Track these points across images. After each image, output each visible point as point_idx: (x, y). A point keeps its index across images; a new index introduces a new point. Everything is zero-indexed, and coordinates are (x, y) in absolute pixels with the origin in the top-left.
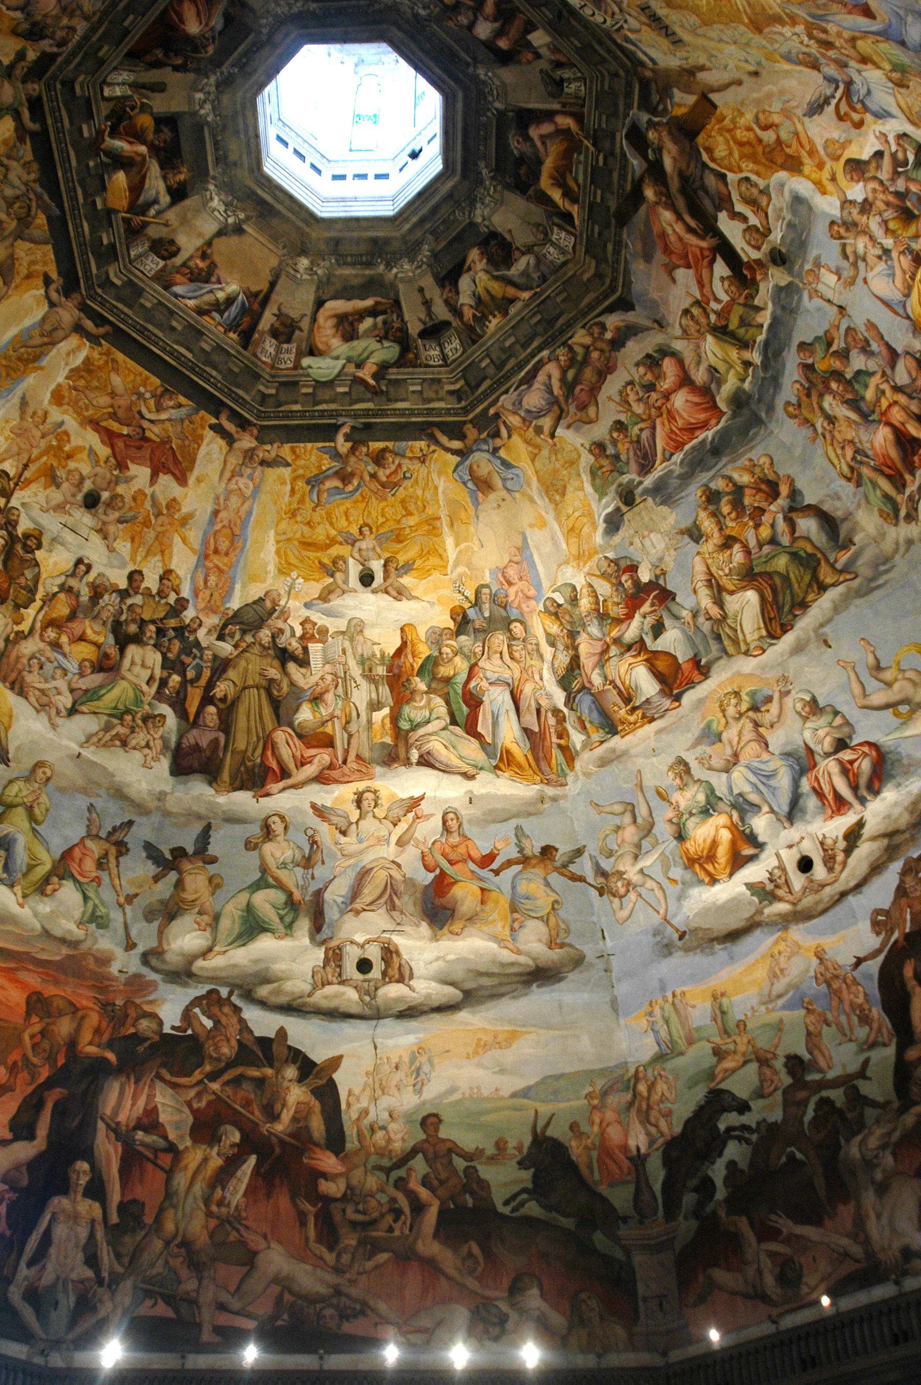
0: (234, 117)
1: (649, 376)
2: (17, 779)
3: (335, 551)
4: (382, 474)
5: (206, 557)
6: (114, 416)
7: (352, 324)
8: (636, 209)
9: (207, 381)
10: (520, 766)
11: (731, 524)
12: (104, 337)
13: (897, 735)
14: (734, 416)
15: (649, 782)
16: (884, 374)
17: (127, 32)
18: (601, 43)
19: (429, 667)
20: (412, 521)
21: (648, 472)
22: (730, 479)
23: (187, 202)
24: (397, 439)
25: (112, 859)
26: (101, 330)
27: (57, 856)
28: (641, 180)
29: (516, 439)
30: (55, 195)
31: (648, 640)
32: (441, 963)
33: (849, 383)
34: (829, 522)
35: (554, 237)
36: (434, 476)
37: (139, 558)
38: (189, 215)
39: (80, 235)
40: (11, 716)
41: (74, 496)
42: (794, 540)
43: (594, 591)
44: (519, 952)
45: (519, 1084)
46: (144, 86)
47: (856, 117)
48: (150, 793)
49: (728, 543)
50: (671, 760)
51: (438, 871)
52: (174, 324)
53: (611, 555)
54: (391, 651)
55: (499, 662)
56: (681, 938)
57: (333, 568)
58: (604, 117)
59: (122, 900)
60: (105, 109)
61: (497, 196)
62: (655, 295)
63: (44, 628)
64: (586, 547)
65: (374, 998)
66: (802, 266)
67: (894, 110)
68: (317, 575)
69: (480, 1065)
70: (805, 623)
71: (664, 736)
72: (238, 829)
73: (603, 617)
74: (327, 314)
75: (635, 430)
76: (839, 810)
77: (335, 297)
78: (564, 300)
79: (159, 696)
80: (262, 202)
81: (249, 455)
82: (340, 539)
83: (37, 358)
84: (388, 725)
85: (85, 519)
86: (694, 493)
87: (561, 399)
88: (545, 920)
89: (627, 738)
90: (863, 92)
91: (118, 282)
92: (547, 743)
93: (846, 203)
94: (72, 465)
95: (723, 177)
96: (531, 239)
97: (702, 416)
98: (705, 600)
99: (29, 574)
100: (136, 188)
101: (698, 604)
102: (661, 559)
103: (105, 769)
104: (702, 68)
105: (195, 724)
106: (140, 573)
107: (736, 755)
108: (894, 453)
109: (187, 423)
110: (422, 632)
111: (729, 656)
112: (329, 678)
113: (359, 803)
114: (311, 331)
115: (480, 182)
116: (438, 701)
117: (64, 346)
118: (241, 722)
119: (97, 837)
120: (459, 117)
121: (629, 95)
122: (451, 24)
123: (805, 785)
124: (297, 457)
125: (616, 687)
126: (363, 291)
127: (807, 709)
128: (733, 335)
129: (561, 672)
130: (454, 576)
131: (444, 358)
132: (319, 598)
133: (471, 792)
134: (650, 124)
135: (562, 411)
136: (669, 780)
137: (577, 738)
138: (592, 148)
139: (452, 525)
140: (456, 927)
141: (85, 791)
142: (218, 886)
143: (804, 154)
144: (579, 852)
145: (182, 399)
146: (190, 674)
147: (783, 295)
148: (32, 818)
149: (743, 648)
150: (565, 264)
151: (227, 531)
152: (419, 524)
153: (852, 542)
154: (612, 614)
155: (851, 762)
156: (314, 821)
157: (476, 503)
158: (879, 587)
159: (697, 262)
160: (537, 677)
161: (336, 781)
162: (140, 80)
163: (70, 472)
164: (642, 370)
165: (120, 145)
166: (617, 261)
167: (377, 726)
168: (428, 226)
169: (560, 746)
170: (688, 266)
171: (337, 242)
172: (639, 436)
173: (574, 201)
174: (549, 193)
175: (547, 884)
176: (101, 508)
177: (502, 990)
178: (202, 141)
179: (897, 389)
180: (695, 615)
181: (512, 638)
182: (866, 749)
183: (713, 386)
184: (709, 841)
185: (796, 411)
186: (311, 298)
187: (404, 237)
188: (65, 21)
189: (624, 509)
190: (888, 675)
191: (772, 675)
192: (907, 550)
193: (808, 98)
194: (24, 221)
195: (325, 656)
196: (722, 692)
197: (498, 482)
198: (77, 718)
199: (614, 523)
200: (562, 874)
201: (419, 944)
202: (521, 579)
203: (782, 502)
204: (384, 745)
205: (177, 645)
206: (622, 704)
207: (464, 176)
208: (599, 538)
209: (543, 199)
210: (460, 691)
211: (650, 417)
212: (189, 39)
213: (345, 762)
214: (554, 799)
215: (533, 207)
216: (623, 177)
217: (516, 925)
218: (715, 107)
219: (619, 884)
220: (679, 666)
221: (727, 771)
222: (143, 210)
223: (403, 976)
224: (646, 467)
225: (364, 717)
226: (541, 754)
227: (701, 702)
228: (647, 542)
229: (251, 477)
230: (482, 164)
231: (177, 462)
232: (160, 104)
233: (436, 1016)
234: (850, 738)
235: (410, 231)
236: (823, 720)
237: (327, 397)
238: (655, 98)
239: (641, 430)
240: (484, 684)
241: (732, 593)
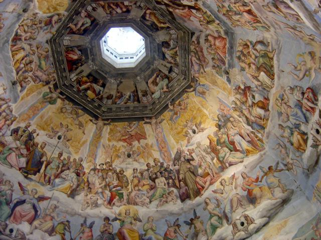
0: (101, 64)
2: (145, 224)
3: (184, 130)
4: (182, 107)
5: (161, 150)
6: (123, 136)
9: (137, 115)
10: (252, 151)
11: (246, 61)
12: (111, 122)
14: (228, 37)
15: (278, 135)
17: (64, 69)
19: (218, 142)
20: (195, 112)
22: (239, 51)
23: (107, 86)
25: (178, 230)
26: (109, 121)
27: (163, 236)
29: (200, 78)
30: (79, 105)
31: (254, 101)
32: (259, 213)
34: (261, 42)
35: (171, 33)
37: (146, 160)
38: (110, 87)
39: (90, 108)
40: (137, 211)
42: (259, 53)
44: (276, 199)
45: (293, 235)
46: (79, 74)
48: (179, 209)
49: (249, 65)
50: (277, 126)
52: (122, 109)
53: (234, 88)
54: (209, 144)
56: (308, 171)
57: (186, 135)
59: (185, 238)
60: (75, 83)
63: (134, 188)
65: (248, 231)
69: (281, 235)
70: (276, 70)
71: (273, 121)
72: (200, 207)
73: (243, 103)
75: (216, 57)
76: (314, 111)
77: (149, 79)
79: (169, 186)
80: (121, 74)
81: (156, 123)
83: (100, 136)
85: (130, 160)
86: (236, 60)
88: (279, 186)
91: (106, 110)
94: (120, 151)
97: (223, 42)
98: (256, 83)
99: (125, 179)
100: (94, 91)
102: (242, 81)
103: (165, 210)
105: (180, 188)
106: (149, 163)
107: (287, 115)
113: (222, 184)
114: (150, 90)
115: (152, 35)
116: (225, 149)
117: (104, 130)
118: (188, 181)
119: (172, 226)
120: (137, 28)
123: (304, 111)
125: (257, 117)
126: (152, 74)
129: (246, 122)
137: (259, 135)
139: (203, 107)
140: (258, 201)
141: (163, 218)
142: (203, 223)
144: (278, 163)
145: (134, 122)
146: (173, 178)
148: (153, 230)
153: (269, 43)
155: (308, 97)
156: (215, 195)
157: (205, 98)
161: (215, 182)
162: (77, 73)
165: (84, 87)
167: (216, 163)
168: (152, 51)
169: (258, 140)
170: (191, 16)
171: (141, 69)
173: (166, 23)
175: (275, 177)
176: (132, 156)
177: (278, 211)
178: (99, 73)
181: (232, 122)
182: (308, 90)
183: (220, 34)
188: (50, 77)
189: (228, 75)
190: (299, 68)
191: (279, 89)
194: (77, 114)
198: (152, 203)
199: (229, 80)
201: (252, 211)
203: (251, 46)
205: (166, 173)
207: (149, 37)
208: (229, 86)
209: (162, 28)
212: (77, 60)
214: (264, 154)
216: (165, 11)
222: (99, 93)
223: (252, 221)
224: (224, 63)
225: (211, 163)
227: (272, 107)
230: (148, 32)
231: (142, 136)
232: (85, 74)
233: (265, 228)
234: (303, 90)
241: (259, 76)
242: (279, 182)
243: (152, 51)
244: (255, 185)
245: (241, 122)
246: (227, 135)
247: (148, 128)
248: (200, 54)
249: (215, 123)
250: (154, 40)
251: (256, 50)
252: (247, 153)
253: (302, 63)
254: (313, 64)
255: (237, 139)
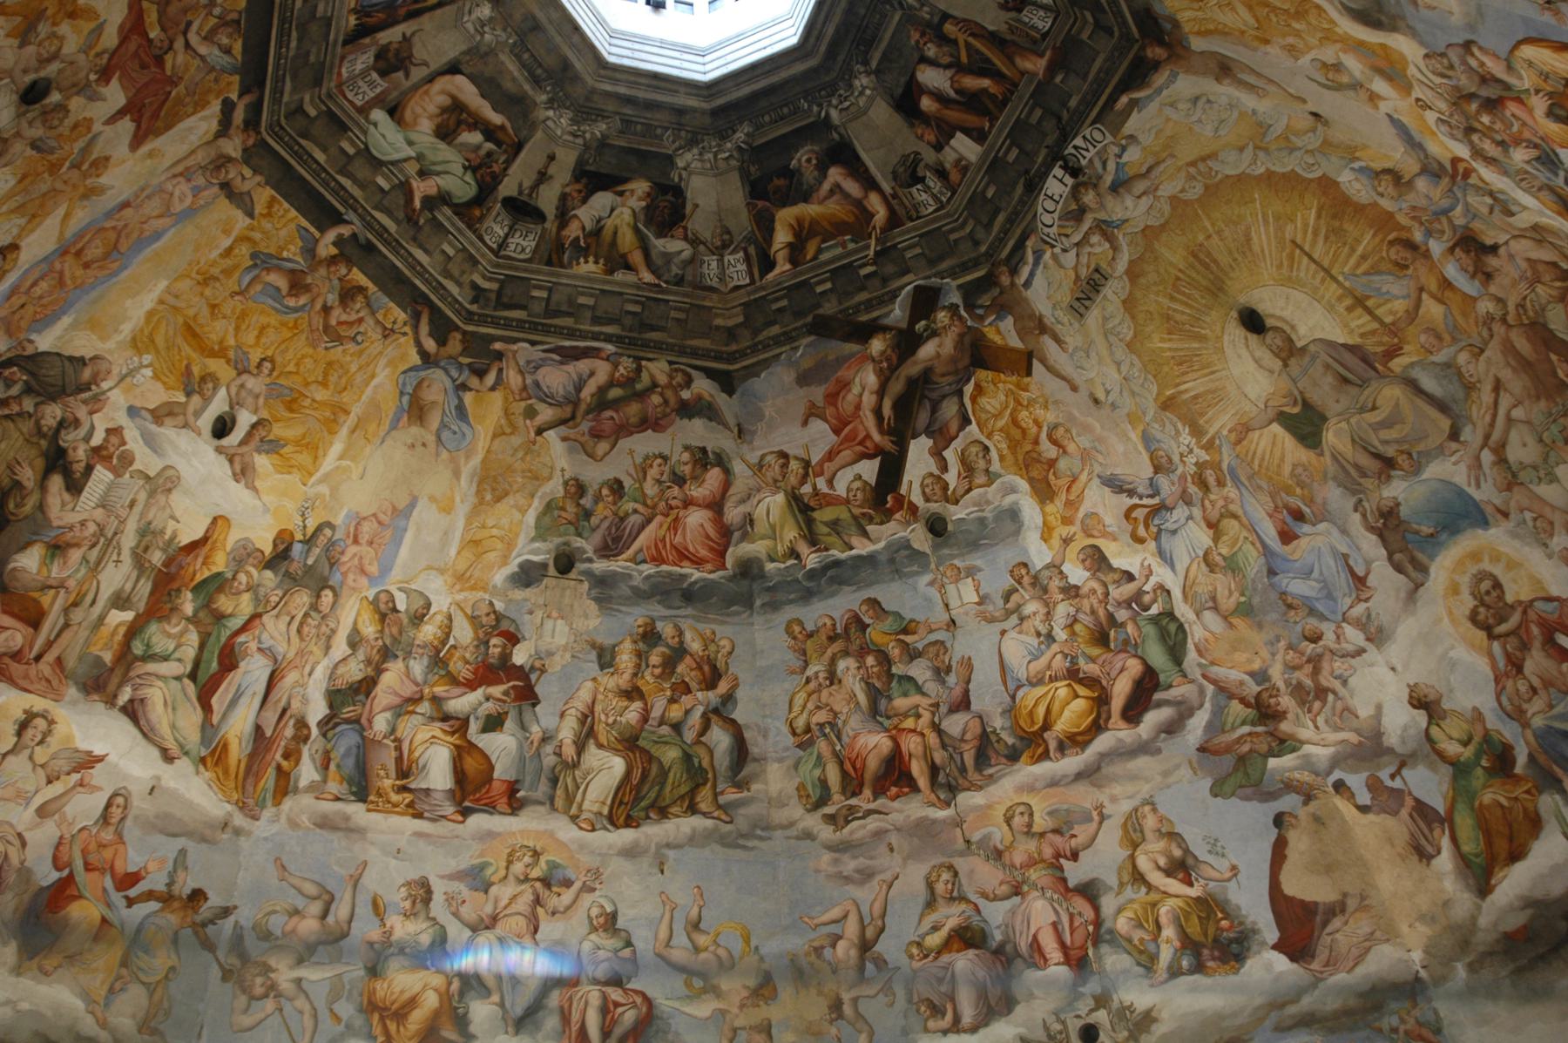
1: (687, 469)
3: (216, 366)
4: (337, 315)
7: (459, 123)
8: (847, 338)
9: (280, 45)
10: (226, 772)
11: (648, 677)
13: (676, 1004)
14: (732, 579)
15: (370, 882)
16: (936, 705)
18: (1011, 221)
19: (212, 587)
20: (321, 395)
21: (607, 557)
22: (681, 634)
24: (383, 287)
28: (885, 329)
29: (497, 398)
31: (474, 727)
33: (891, 676)
36: (382, 362)
41: (25, 71)
42: (698, 742)
43: (450, 628)
44: (103, 1024)
47: (1141, 531)
50: (414, 875)
51: (66, 873)
53: (499, 606)
54: (185, 539)
55: (282, 626)
57: (196, 385)
58: (918, 251)
61: (722, 164)
62: (768, 411)
64: (477, 573)
66: (953, 557)
67: (1181, 567)
68: (171, 380)
70: (654, 832)
71: (421, 843)
73: (438, 661)
74: (449, 87)
77: (472, 78)
78: (678, 320)
81: (223, 161)
82: (231, 354)
84: (119, 637)
86: (636, 617)
87: (583, 407)
88: (151, 989)
89: (374, 815)
90: (1169, 526)
92: (268, 757)
93: (1055, 567)
94: (65, 28)
95: (966, 421)
96: (706, 235)
97: (703, 553)
98: (567, 732)
101: (557, 730)
102: (550, 654)
104: (1058, 340)
108: (873, 764)
109: (212, 76)
110: (233, 537)
111: (553, 809)
112: (92, 528)
113: (23, 727)
114: (415, 88)
115: (723, 136)
116: (193, 638)
120: (784, 74)
121: (965, 268)
122: (915, 36)
124: (269, 215)
125: (399, 749)
127: (602, 920)
128: (810, 522)
129: (340, 684)
130: (311, 492)
131: (503, 244)
132: (152, 412)
133: (158, 778)
134: (953, 309)
135: (573, 417)
136: (397, 897)
137: (307, 772)
138: (871, 253)
139: (353, 431)
143: (1064, 496)
144: (226, 912)
145: (238, 47)
147: (905, 553)
149: (574, 811)
150: (712, 289)
151: (112, 236)
152: (324, 404)
154: (451, 667)
155: (617, 1005)
157: (394, 426)
158: (744, 847)
159: (850, 439)
160: (308, 669)
161: (12, 682)
163: (54, 35)
164: (686, 456)
166: (766, 347)
167: (105, 631)
168: (628, 111)
169: (279, 768)
170: (837, 432)
171: (536, 27)
172: (627, 515)
174: (778, 226)
179: (936, 728)
180: (545, 739)
181: (314, 607)
182: (639, 1000)
183: (737, 535)
184: (407, 996)
185: (801, 639)
186: (452, 54)
187: (593, 91)
189: (552, 571)
190: (702, 940)
191: (586, 860)
192: (798, 838)
193: (1118, 471)
195: (107, 494)
196: (521, 841)
197: (434, 421)
199: (528, 576)
200: (196, 933)
202: (370, 543)
204: (98, 661)
206: (393, 774)
207: (715, 113)
208: (499, 577)
209: (766, 225)
210: (223, 639)
211: (654, 507)
213: (38, 658)
214: (238, 832)
215: (744, 215)
216: (869, 305)
217: (118, 986)
218: (1029, 373)
219: (259, 980)
220: (490, 780)
221: (475, 929)
224: (610, 548)
225: (101, 604)
226: (255, 768)
227: (490, 835)
228: (549, 624)
229: (197, 191)
234: (629, 980)
235: (608, 94)
236: (612, 943)
237: (359, 175)
238: (985, 300)
239: (635, 511)
240: (253, 646)
241: (600, 746)
242: (166, 977)
243: (628, 111)
244: (105, 890)
245: (328, 648)
246: (256, 616)
247: (200, 125)
248: (633, 410)
249: (290, 527)
250: (692, 142)
251: (706, 727)
252: (213, 757)
253: (721, 952)
254: (736, 1000)
255: (253, 671)
